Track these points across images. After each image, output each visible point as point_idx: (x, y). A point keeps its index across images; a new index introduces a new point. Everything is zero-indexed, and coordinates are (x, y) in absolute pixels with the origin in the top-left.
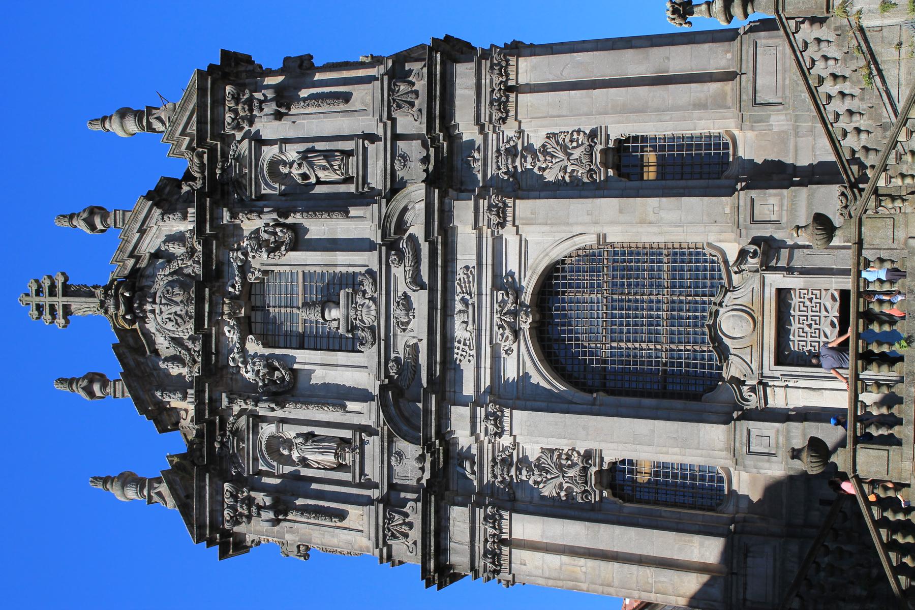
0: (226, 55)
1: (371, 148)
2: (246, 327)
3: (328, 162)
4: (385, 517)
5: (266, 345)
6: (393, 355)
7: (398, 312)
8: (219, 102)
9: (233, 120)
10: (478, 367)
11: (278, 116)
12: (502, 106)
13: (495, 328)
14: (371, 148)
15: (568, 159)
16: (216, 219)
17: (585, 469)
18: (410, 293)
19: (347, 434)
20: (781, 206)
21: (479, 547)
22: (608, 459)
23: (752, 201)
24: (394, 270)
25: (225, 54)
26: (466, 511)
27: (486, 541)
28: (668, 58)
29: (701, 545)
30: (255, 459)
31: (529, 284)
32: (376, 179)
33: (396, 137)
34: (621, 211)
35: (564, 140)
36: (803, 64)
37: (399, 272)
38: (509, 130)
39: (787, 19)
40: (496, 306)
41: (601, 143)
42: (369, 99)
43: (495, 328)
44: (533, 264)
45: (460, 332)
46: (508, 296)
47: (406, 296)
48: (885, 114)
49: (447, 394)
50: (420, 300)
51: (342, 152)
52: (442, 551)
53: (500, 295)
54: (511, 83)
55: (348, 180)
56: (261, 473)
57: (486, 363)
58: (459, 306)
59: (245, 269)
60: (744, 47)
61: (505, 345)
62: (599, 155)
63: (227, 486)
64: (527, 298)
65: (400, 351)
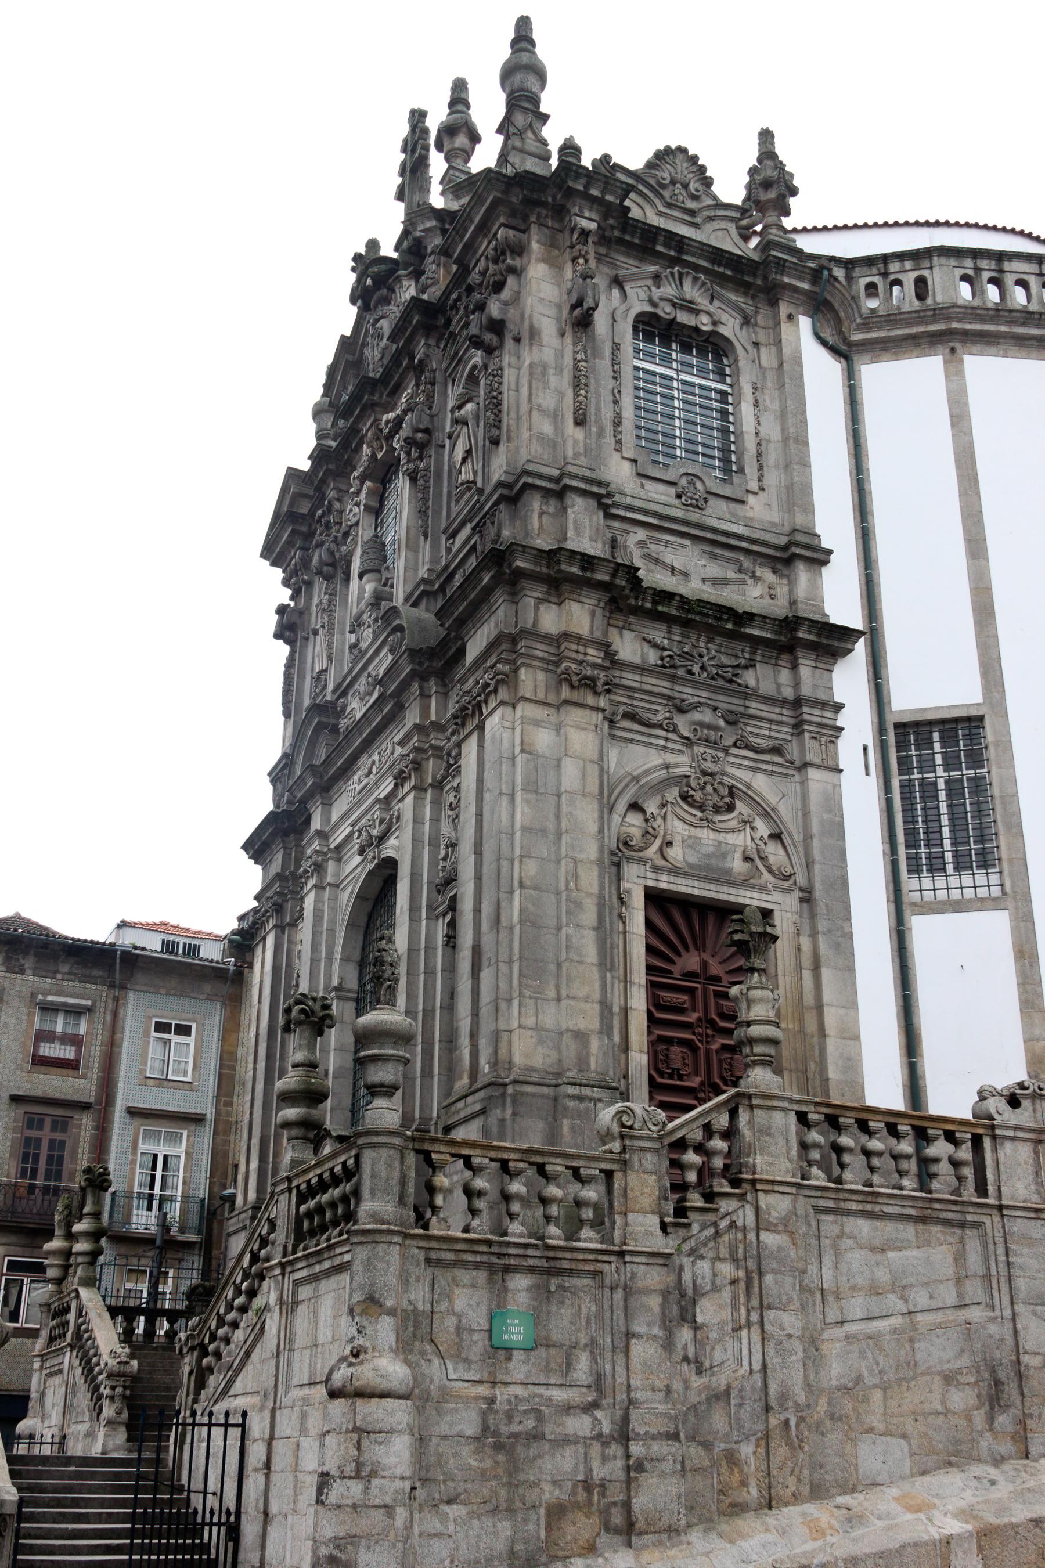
46: (381, 823)
49: (332, 792)
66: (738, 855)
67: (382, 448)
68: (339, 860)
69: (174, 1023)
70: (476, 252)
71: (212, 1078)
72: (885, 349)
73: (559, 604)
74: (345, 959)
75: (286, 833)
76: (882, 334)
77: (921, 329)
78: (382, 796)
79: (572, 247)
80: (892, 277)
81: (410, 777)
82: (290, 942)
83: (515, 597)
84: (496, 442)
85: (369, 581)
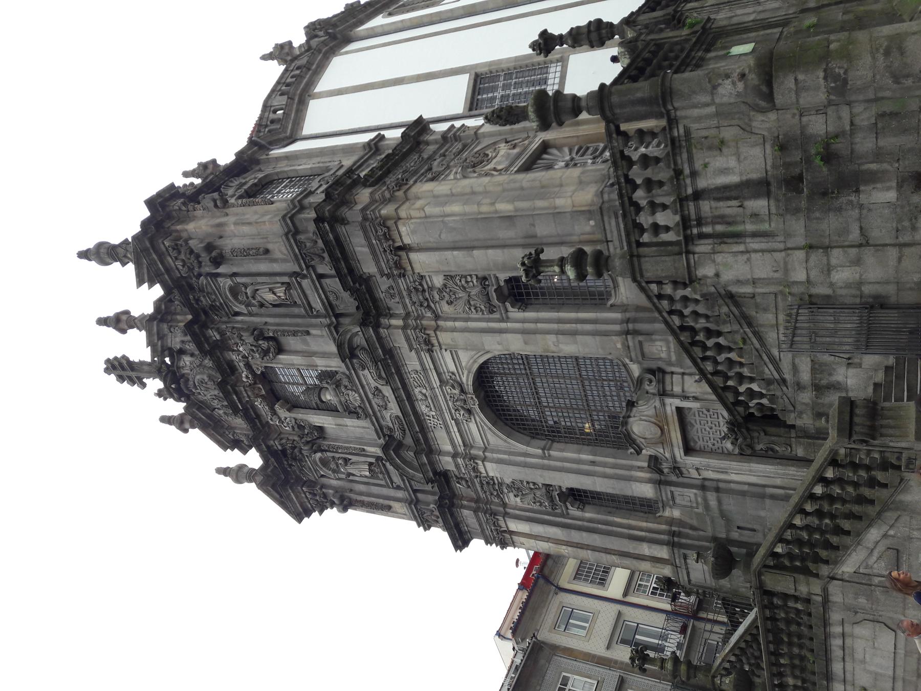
0: (150, 203)
3: (274, 293)
4: (418, 512)
5: (289, 410)
6: (383, 423)
7: (376, 400)
9: (183, 266)
10: (448, 433)
13: (453, 411)
15: (469, 296)
18: (380, 387)
19: (373, 460)
20: (669, 348)
23: (640, 343)
24: (361, 373)
25: (150, 203)
27: (492, 531)
28: (533, 225)
29: (649, 548)
30: (316, 471)
32: (317, 305)
33: (320, 277)
34: (526, 343)
35: (460, 281)
36: (672, 323)
39: (648, 282)
40: (448, 398)
41: (493, 285)
42: (283, 249)
43: (453, 411)
44: (467, 364)
47: (377, 388)
48: (766, 370)
49: (433, 447)
50: (387, 391)
51: (283, 283)
53: (448, 389)
54: (399, 244)
56: (322, 476)
60: (606, 218)
62: (494, 294)
64: (470, 388)
66: (511, 151)
67: (259, 388)
68: (472, 447)
69: (559, 686)
70: (172, 268)
71: (598, 669)
72: (299, 124)
73: (356, 204)
74: (528, 445)
75: (452, 505)
76: (291, 122)
77: (295, 106)
78: (438, 384)
79: (188, 211)
80: (269, 123)
81: (428, 335)
82: (514, 509)
83: (344, 221)
84: (267, 251)
85: (325, 395)
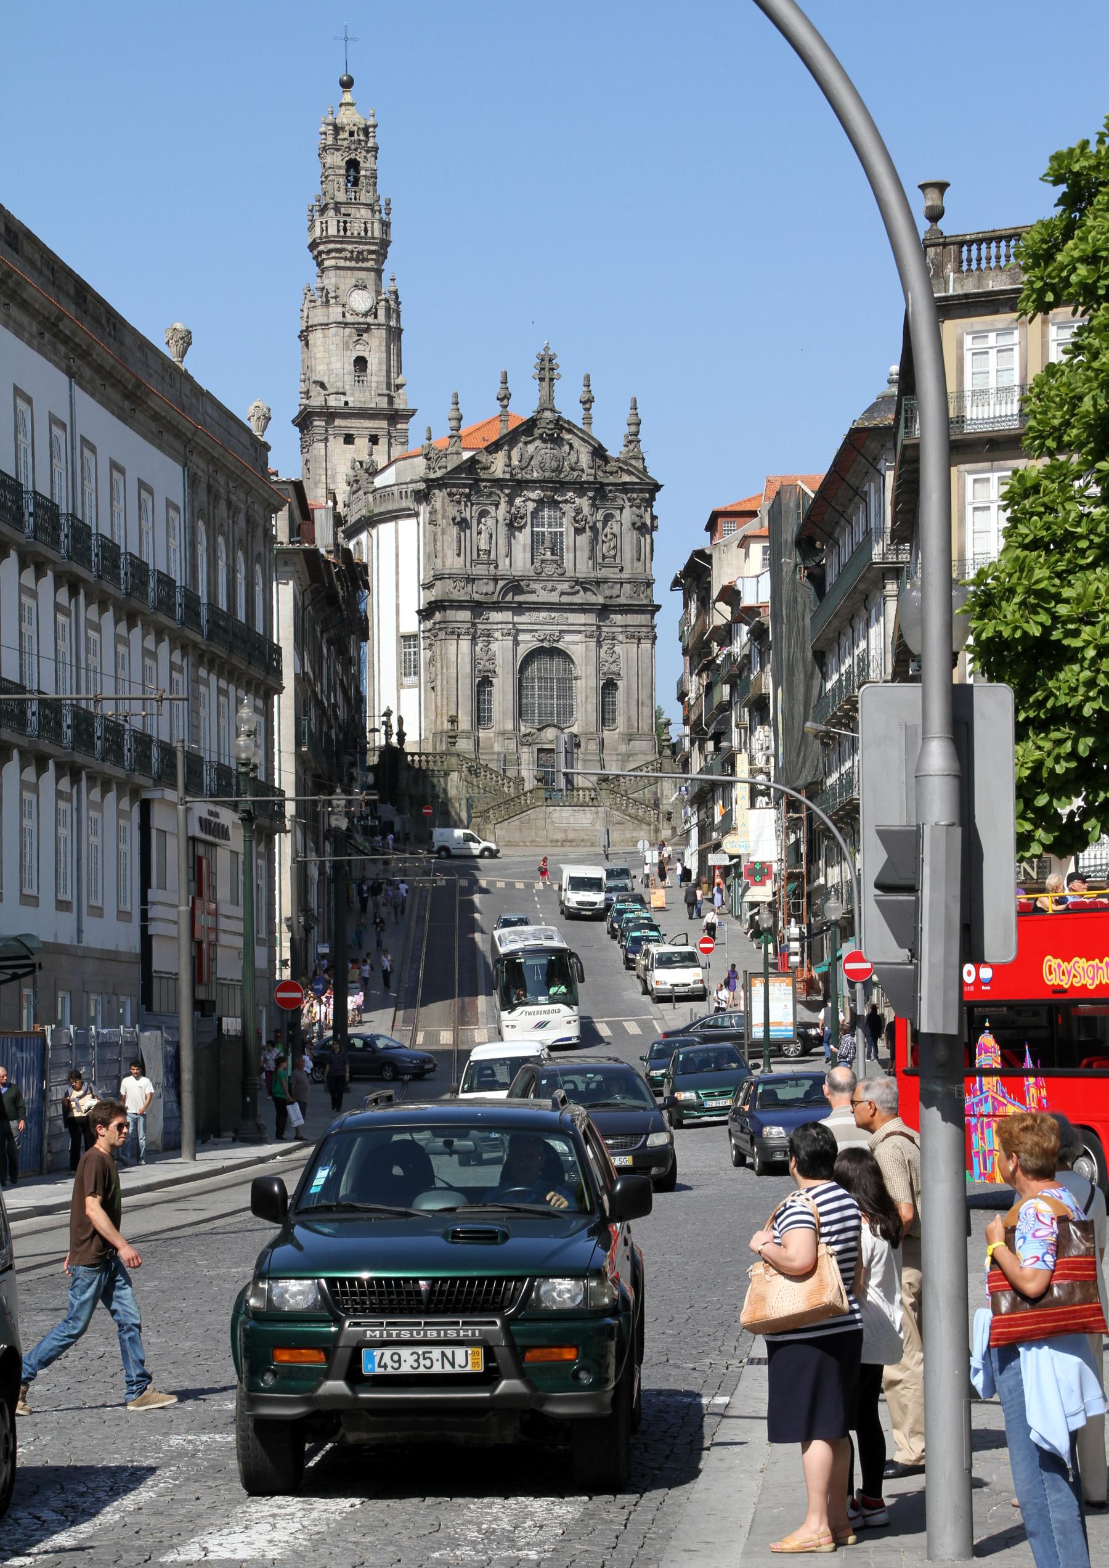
1: (617, 570)
2: (540, 502)
8: (642, 491)
11: (634, 524)
12: (633, 637)
14: (617, 570)
16: (589, 489)
17: (489, 671)
19: (493, 556)
21: (455, 625)
22: (494, 680)
26: (468, 619)
31: (560, 645)
33: (622, 583)
37: (565, 586)
38: (621, 637)
45: (543, 615)
52: (452, 607)
55: (604, 557)
57: (530, 627)
58: (553, 615)
59: (566, 501)
61: (536, 635)
63: (467, 490)
64: (555, 645)
65: (533, 586)
